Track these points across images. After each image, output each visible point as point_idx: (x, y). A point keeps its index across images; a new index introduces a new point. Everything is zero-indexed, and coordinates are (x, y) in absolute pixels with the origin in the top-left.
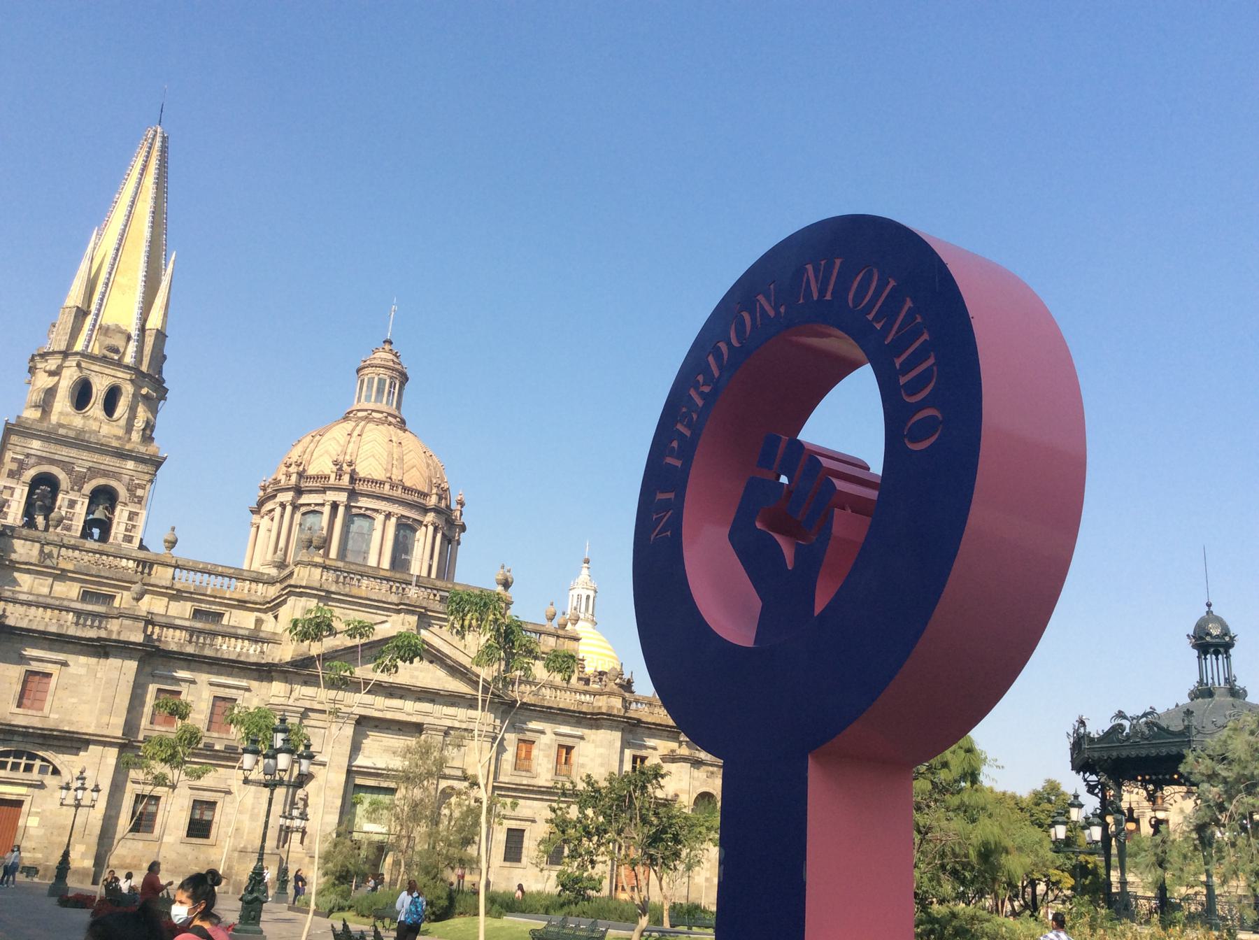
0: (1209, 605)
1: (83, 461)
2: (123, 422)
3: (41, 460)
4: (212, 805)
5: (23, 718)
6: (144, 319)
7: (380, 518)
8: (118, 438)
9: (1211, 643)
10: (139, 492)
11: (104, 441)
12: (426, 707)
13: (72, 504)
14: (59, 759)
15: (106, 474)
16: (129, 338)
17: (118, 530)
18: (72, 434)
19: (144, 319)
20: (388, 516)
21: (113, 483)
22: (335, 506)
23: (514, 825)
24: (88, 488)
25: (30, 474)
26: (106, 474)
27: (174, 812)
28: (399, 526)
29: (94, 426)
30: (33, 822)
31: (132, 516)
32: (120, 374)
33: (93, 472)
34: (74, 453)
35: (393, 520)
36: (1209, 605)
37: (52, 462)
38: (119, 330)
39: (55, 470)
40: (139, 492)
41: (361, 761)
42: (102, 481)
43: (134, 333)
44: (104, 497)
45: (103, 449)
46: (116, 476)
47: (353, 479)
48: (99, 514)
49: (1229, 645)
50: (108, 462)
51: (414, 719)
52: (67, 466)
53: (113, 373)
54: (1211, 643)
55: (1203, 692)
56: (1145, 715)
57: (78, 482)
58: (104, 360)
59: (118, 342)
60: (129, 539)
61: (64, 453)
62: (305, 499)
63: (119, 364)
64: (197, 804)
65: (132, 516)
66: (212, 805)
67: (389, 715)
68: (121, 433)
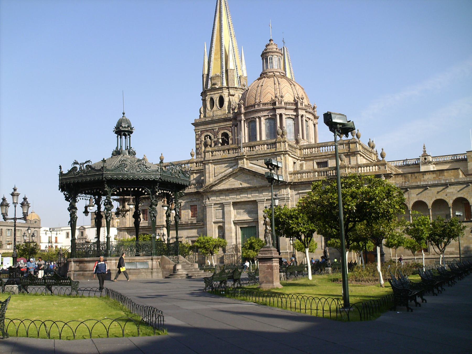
0: (124, 114)
1: (216, 126)
9: (123, 130)
11: (220, 117)
18: (210, 119)
21: (226, 131)
26: (223, 128)
29: (215, 113)
32: (220, 92)
34: (212, 126)
35: (262, 118)
36: (124, 114)
37: (207, 131)
42: (222, 132)
51: (252, 199)
53: (217, 92)
54: (123, 130)
57: (216, 134)
67: (243, 200)
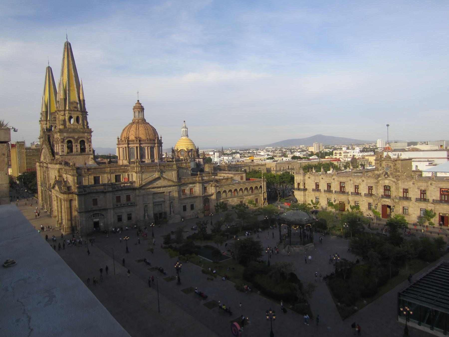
2: (82, 124)
3: (67, 137)
4: (131, 214)
5: (95, 208)
6: (79, 97)
7: (146, 148)
8: (82, 128)
10: (90, 140)
12: (164, 188)
13: (77, 146)
14: (103, 213)
15: (81, 137)
16: (77, 103)
17: (87, 150)
19: (79, 97)
20: (148, 147)
21: (84, 139)
22: (137, 147)
23: (184, 205)
24: (79, 141)
25: (66, 141)
27: (125, 218)
28: (150, 148)
30: (102, 224)
31: (90, 146)
33: (79, 138)
38: (75, 102)
39: (71, 139)
40: (90, 140)
41: (154, 200)
42: (81, 139)
43: (78, 102)
44: (82, 143)
45: (79, 132)
46: (84, 137)
47: (140, 141)
48: (83, 147)
50: (81, 135)
52: (73, 138)
58: (74, 110)
59: (75, 105)
60: (90, 151)
61: (71, 135)
62: (129, 146)
63: (77, 111)
64: (128, 215)
65: (90, 146)
66: (131, 214)
68: (82, 127)
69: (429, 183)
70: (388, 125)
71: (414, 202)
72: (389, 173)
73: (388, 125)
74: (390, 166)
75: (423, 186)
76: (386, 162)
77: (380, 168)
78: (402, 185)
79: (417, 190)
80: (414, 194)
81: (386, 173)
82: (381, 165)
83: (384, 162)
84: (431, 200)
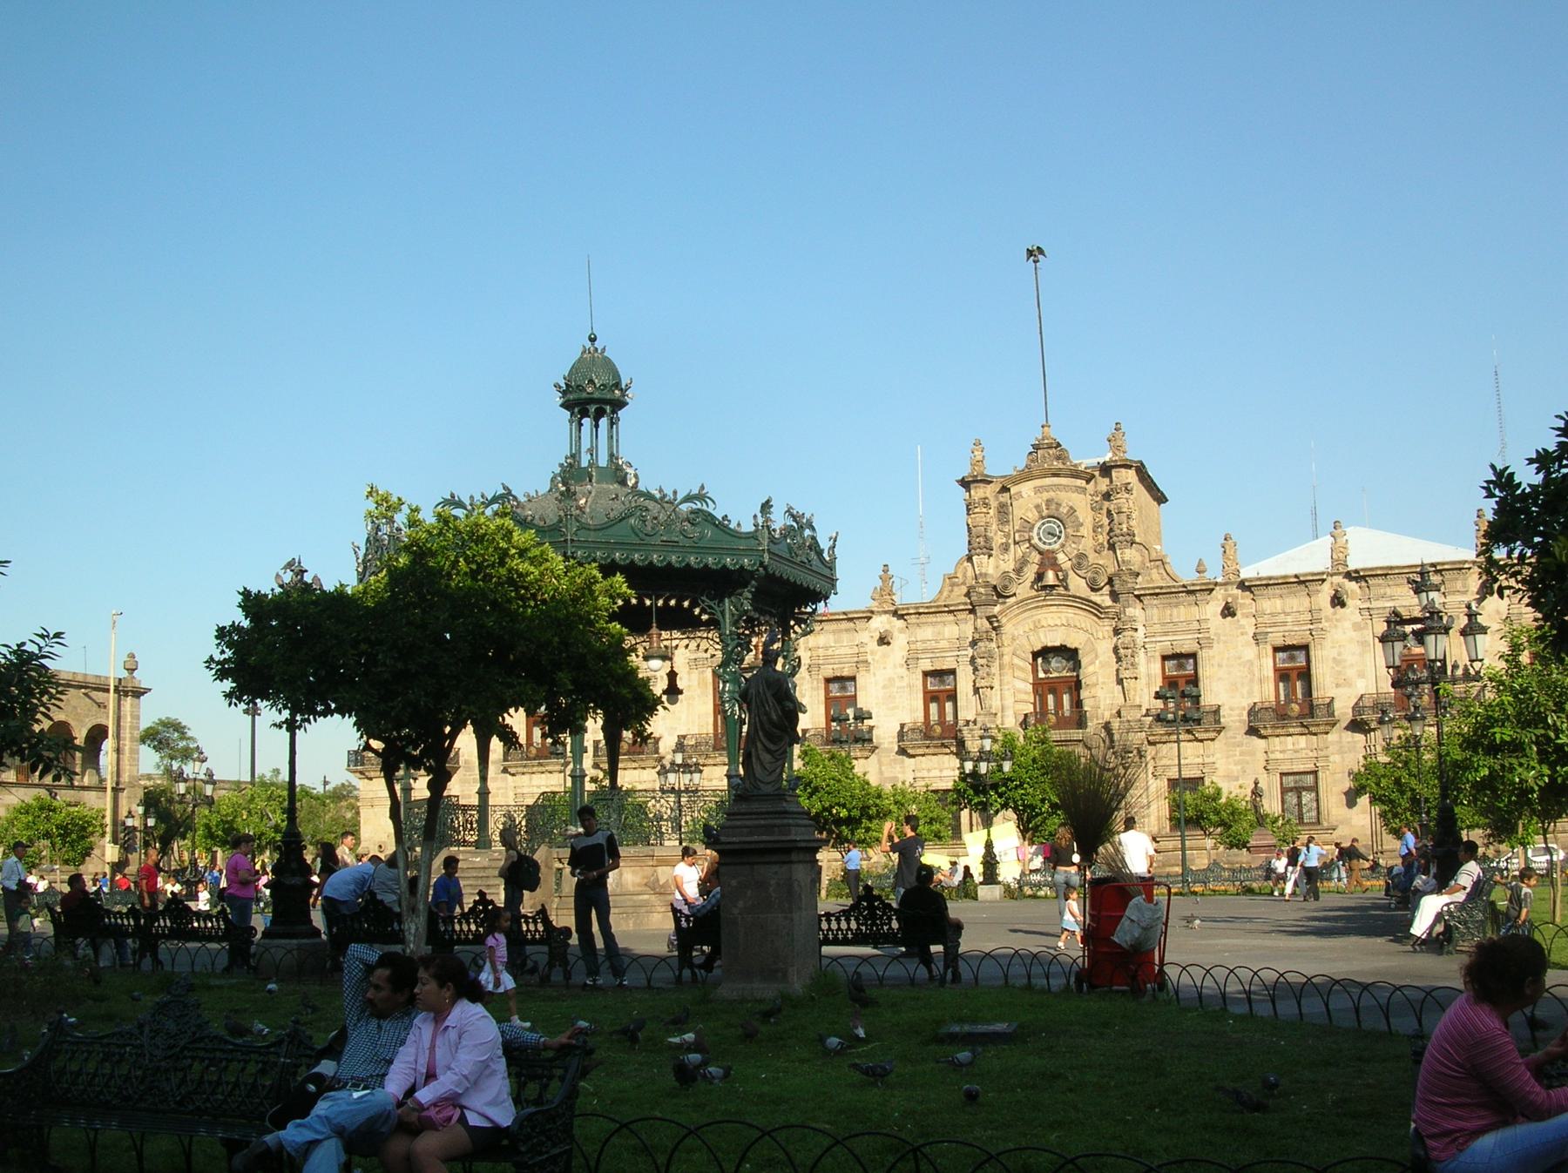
9: (593, 397)
49: (619, 404)
54: (593, 397)
55: (572, 474)
56: (495, 500)
69: (1326, 592)
70: (1034, 253)
71: (1241, 737)
72: (1061, 557)
73: (1034, 253)
74: (1072, 510)
75: (1287, 615)
76: (1038, 490)
77: (998, 539)
78: (1155, 629)
79: (1250, 652)
80: (1236, 678)
81: (1048, 560)
82: (1003, 512)
83: (1026, 488)
84: (1343, 710)
